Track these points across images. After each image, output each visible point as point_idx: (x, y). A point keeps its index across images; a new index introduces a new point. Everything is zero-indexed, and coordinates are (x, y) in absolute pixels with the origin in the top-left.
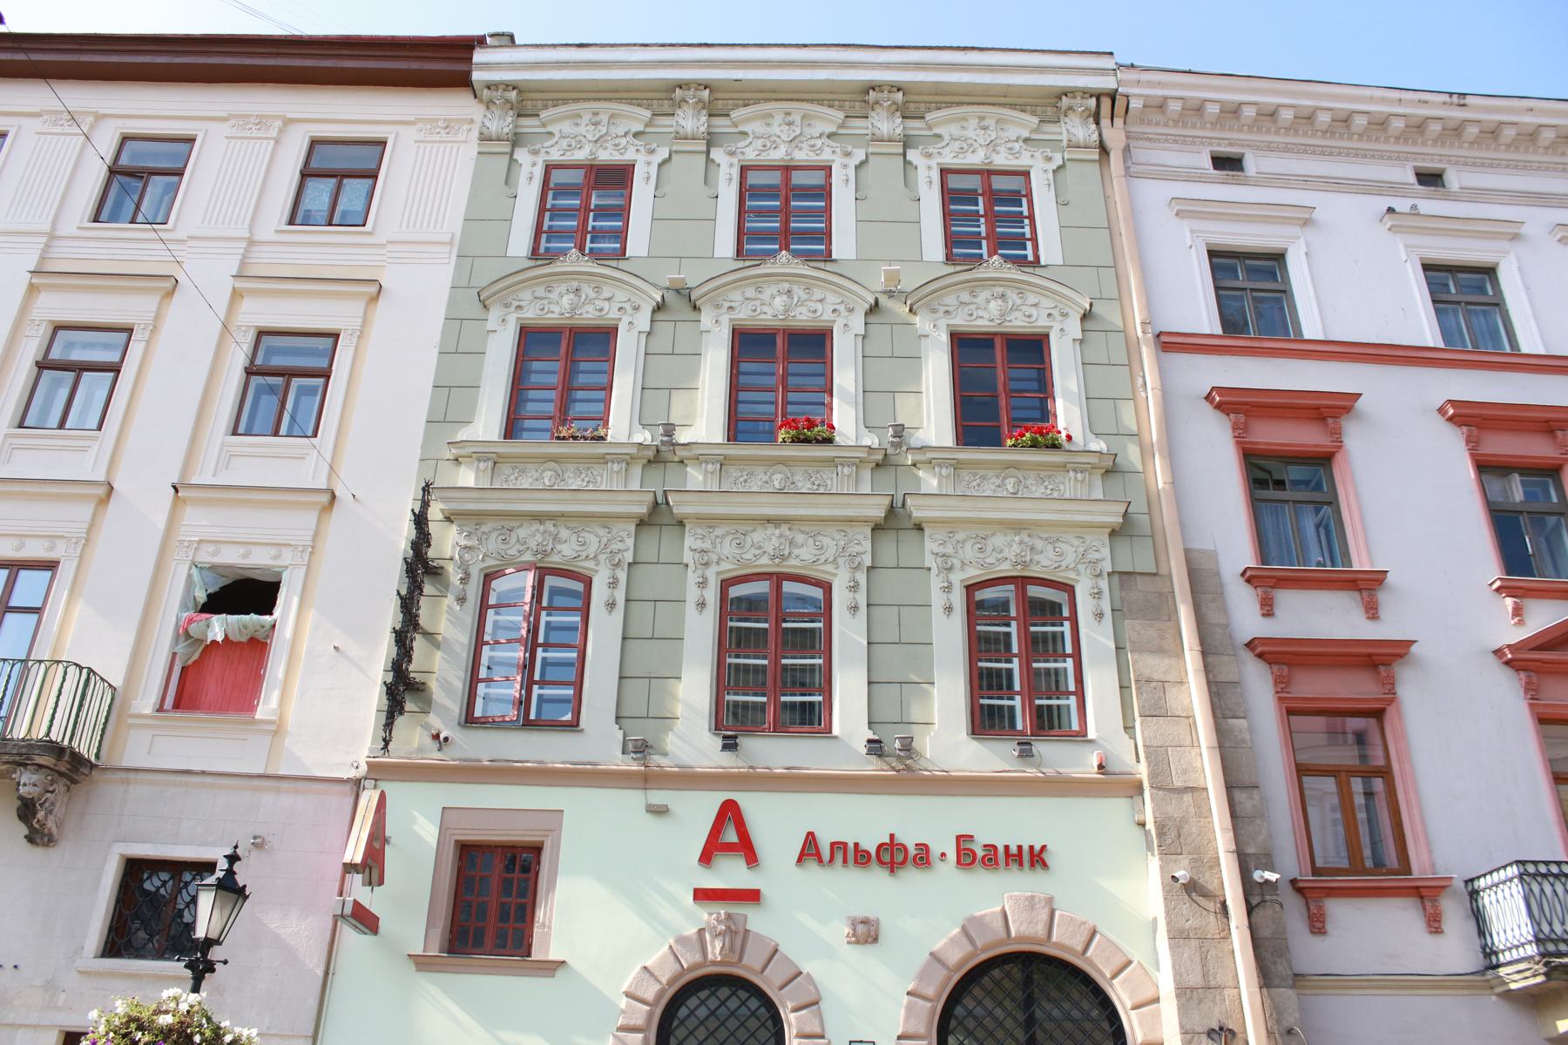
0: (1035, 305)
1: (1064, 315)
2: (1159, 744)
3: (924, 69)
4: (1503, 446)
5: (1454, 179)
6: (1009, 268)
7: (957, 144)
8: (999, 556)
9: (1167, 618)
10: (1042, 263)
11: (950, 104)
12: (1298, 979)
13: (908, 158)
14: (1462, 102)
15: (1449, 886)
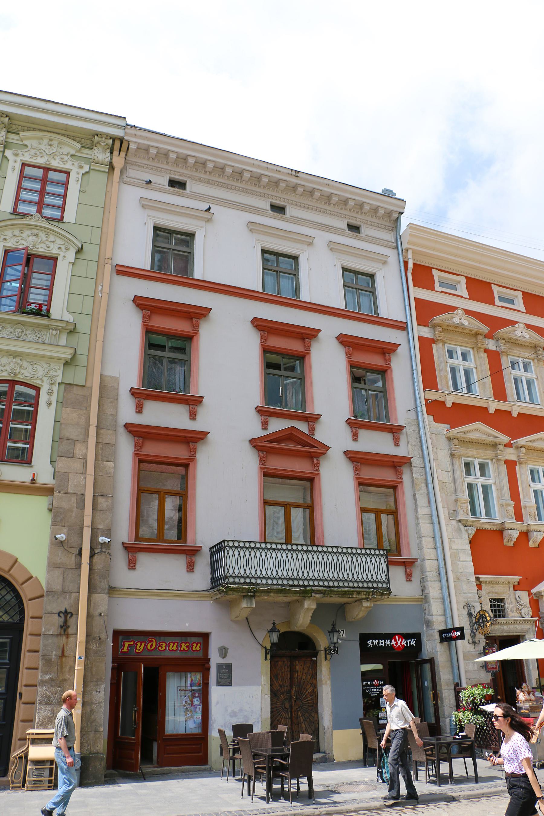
0: (53, 242)
1: (67, 249)
2: (65, 471)
3: (22, 107)
4: (276, 342)
5: (291, 211)
6: (43, 221)
7: (33, 152)
8: (3, 368)
9: (85, 409)
10: (64, 221)
11: (35, 130)
12: (112, 590)
13: (5, 154)
14: (297, 175)
15: (200, 550)
